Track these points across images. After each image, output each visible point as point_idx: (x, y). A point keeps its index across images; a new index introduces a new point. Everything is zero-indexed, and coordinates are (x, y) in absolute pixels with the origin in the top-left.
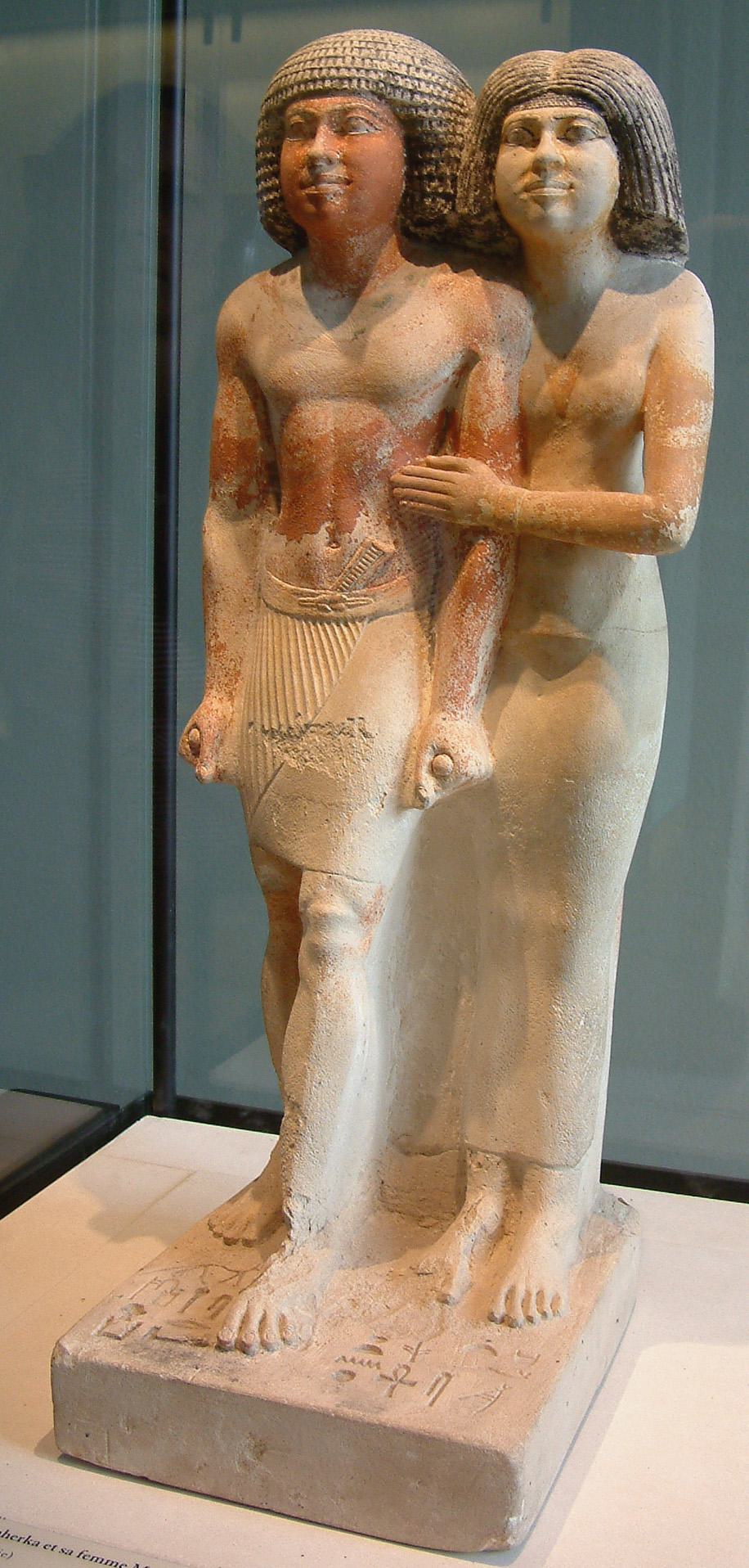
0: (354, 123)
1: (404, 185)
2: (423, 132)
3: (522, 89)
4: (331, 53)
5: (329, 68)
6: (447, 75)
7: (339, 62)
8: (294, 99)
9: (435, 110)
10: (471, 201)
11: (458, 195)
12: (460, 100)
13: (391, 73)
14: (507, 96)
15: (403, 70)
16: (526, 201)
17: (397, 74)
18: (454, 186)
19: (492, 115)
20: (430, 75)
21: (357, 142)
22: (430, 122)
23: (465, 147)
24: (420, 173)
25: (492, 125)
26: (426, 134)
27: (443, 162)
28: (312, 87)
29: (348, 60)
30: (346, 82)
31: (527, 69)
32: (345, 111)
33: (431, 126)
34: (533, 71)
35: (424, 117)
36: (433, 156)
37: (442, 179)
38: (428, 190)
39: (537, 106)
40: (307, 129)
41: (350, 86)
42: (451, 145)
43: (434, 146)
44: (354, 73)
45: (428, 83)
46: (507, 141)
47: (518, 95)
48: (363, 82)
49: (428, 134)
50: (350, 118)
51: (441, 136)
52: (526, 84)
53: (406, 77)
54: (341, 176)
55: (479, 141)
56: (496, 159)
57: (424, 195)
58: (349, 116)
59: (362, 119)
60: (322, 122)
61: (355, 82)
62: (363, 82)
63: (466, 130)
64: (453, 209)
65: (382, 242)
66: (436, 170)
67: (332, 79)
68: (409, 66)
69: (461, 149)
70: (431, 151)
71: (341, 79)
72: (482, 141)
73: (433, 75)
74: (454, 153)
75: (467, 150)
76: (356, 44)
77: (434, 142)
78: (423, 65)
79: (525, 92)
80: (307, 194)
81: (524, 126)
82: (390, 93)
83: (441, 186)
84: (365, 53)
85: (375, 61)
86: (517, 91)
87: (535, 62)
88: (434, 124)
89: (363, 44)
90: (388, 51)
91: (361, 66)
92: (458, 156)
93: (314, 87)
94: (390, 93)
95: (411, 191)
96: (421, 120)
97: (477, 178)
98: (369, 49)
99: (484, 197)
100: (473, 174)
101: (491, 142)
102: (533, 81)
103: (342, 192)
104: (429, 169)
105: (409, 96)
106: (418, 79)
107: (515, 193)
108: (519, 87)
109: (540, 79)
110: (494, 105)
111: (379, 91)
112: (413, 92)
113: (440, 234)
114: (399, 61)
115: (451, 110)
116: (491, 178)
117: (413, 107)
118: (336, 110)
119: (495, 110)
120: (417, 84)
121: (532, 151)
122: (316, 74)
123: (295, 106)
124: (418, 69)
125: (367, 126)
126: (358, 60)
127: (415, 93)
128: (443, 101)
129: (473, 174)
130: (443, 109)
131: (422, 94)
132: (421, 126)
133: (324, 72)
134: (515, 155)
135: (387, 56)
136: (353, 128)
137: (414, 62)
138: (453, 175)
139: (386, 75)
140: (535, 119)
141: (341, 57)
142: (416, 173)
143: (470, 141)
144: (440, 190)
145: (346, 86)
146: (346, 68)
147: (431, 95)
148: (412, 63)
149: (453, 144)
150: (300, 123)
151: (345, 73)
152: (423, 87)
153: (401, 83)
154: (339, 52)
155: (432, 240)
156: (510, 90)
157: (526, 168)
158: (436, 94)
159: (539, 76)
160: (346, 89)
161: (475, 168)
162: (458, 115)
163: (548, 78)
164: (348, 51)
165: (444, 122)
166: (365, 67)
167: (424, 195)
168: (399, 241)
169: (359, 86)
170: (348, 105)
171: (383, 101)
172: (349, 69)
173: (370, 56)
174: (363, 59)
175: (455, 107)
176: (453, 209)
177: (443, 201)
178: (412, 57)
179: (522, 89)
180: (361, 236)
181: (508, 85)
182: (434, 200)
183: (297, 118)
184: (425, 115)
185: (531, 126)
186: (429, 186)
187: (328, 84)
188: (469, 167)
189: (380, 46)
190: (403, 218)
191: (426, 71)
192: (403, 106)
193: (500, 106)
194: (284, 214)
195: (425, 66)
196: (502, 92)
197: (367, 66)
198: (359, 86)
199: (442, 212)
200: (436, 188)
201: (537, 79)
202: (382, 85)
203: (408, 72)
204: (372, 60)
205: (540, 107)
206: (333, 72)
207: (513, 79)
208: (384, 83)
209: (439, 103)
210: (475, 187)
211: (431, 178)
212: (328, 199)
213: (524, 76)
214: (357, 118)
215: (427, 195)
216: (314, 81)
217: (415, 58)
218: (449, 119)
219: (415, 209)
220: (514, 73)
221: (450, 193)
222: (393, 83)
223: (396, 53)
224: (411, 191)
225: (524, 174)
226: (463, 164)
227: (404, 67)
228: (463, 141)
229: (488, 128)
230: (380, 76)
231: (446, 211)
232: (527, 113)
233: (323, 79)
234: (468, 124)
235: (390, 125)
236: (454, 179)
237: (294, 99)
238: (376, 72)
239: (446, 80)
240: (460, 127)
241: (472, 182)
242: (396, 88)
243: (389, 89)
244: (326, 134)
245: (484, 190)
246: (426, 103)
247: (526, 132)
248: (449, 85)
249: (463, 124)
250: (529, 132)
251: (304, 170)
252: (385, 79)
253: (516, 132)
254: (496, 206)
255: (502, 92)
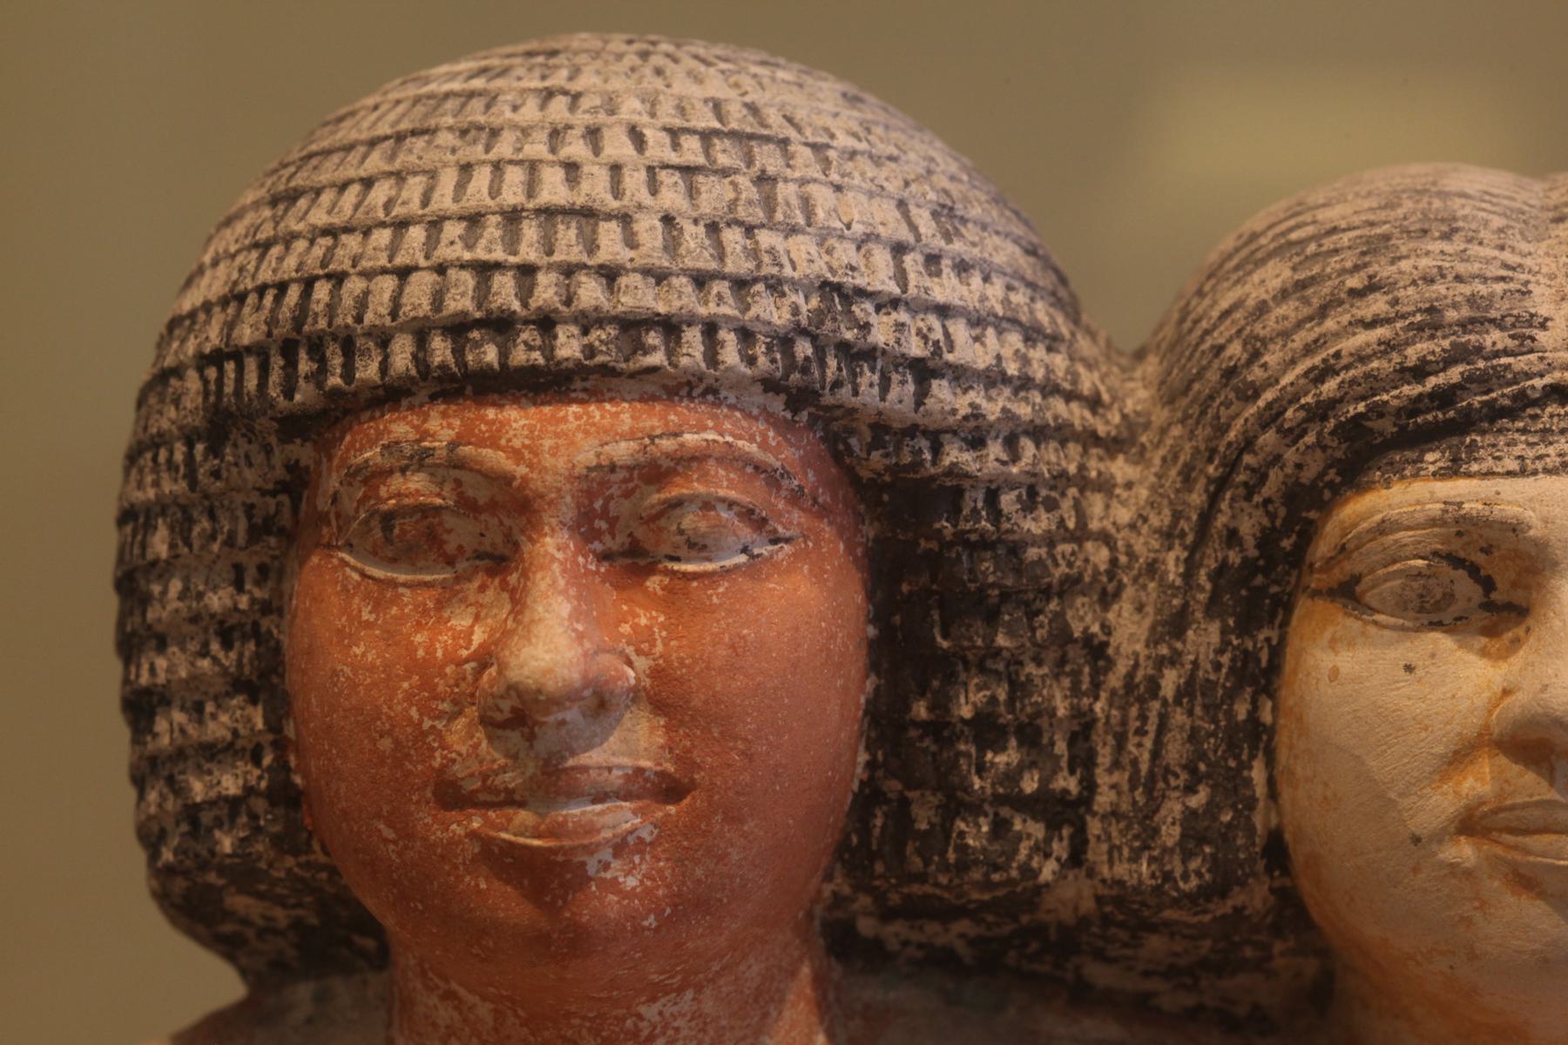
0: (691, 520)
1: (863, 757)
2: (961, 538)
3: (1432, 382)
4: (554, 190)
5: (569, 270)
6: (1025, 263)
7: (610, 242)
8: (391, 395)
9: (1011, 443)
10: (1171, 834)
11: (1104, 799)
12: (1088, 382)
13: (838, 288)
14: (1361, 407)
15: (880, 277)
16: (1468, 874)
17: (861, 293)
18: (1083, 761)
19: (1275, 477)
20: (976, 280)
21: (713, 609)
22: (992, 497)
23: (1129, 592)
24: (941, 705)
25: (1272, 516)
26: (967, 544)
27: (1039, 662)
28: (491, 354)
29: (649, 229)
30: (653, 338)
31: (1440, 288)
32: (654, 472)
33: (996, 514)
34: (1472, 300)
35: (967, 476)
36: (1002, 640)
37: (1030, 736)
38: (977, 783)
39: (1513, 465)
40: (460, 532)
41: (670, 354)
42: (1071, 586)
43: (1005, 596)
44: (680, 298)
45: (978, 322)
46: (1348, 593)
47: (1414, 407)
48: (728, 338)
49: (985, 544)
50: (678, 503)
51: (1032, 553)
52: (1448, 361)
53: (895, 303)
54: (645, 763)
55: (1202, 577)
56: (1277, 652)
57: (957, 804)
58: (673, 492)
59: (731, 504)
60: (549, 520)
61: (693, 338)
62: (728, 338)
63: (1124, 515)
64: (1077, 857)
65: (766, 998)
66: (1011, 700)
67: (587, 322)
68: (899, 249)
69: (1107, 599)
70: (992, 618)
71: (633, 326)
72: (1215, 576)
73: (986, 279)
74: (1082, 617)
75: (1140, 608)
76: (659, 148)
77: (1009, 582)
78: (948, 237)
79: (1444, 397)
80: (473, 835)
81: (1456, 546)
82: (837, 384)
83: (1033, 765)
84: (713, 194)
85: (765, 238)
86: (1410, 390)
87: (1463, 256)
88: (1008, 501)
89: (692, 151)
90: (803, 182)
91: (713, 265)
92: (1095, 628)
93: (504, 354)
94: (837, 384)
95: (893, 786)
96: (951, 490)
97: (1194, 736)
98: (725, 173)
99: (1226, 817)
100: (1179, 717)
101: (1259, 580)
102: (1479, 349)
103: (646, 834)
104: (980, 697)
105: (911, 387)
106: (943, 311)
107: (1417, 840)
108: (1419, 372)
109: (1511, 344)
110: (1293, 435)
111: (795, 377)
112: (923, 372)
113: (972, 942)
114: (858, 229)
115: (1062, 433)
116: (1258, 737)
117: (925, 433)
118: (613, 468)
119: (1290, 455)
120: (938, 335)
121: (1484, 653)
122: (505, 290)
123: (401, 428)
124: (932, 261)
125: (746, 534)
126: (693, 236)
127: (936, 374)
128: (1037, 397)
129: (1179, 717)
130: (1039, 433)
131: (961, 376)
132: (955, 512)
133: (546, 291)
134: (1409, 668)
135: (807, 205)
136: (691, 545)
137: (913, 228)
138: (1076, 713)
139: (815, 302)
140: (1515, 528)
141: (609, 217)
142: (921, 710)
143: (1152, 568)
144: (1030, 785)
145: (657, 358)
146: (646, 272)
147: (993, 378)
148: (911, 239)
149: (1078, 579)
150: (438, 510)
151: (638, 296)
152: (969, 351)
153: (881, 333)
154: (595, 187)
155: (942, 960)
156: (1375, 383)
157: (1471, 732)
158: (1012, 369)
159: (1498, 324)
160: (653, 370)
161: (1180, 694)
162: (1085, 452)
163: (1541, 336)
164: (635, 182)
165: (1044, 492)
166: (730, 267)
167: (957, 804)
168: (819, 980)
169: (712, 357)
170: (667, 444)
171: (804, 416)
172: (660, 277)
173: (741, 213)
174: (713, 228)
175: (1077, 414)
176: (1077, 857)
177: (1037, 830)
178: (902, 204)
179: (1432, 382)
180: (689, 994)
181: (1361, 358)
182: (1000, 828)
183: (416, 484)
184: (973, 467)
185: (1487, 551)
186: (981, 769)
187: (568, 346)
188: (1154, 686)
189: (766, 156)
190: (846, 890)
191: (962, 267)
192: (882, 430)
193: (1320, 445)
194: (290, 861)
195: (957, 246)
196: (1330, 387)
197: (737, 264)
198: (712, 357)
199: (1036, 874)
200: (1012, 776)
201: (1495, 338)
202: (804, 348)
203: (901, 277)
204: (749, 230)
205: (1523, 472)
206: (590, 292)
207: (1382, 332)
208: (814, 339)
209: (1023, 411)
210: (1184, 776)
211: (987, 730)
212: (592, 869)
213: (1432, 321)
214: (707, 505)
215: (975, 810)
216: (501, 325)
217: (914, 211)
218: (1063, 474)
219: (917, 863)
220: (1377, 305)
221: (1065, 791)
222: (849, 335)
223: (838, 188)
224: (893, 786)
225: (1460, 756)
226: (1122, 667)
227: (882, 258)
228: (1114, 562)
229: (1248, 527)
230: (795, 311)
231: (1048, 870)
232: (1468, 492)
233: (546, 323)
234: (1129, 485)
235: (823, 512)
236: (1082, 730)
237: (391, 395)
238: (776, 286)
239: (1029, 292)
240: (1096, 504)
241: (1175, 751)
242: (857, 355)
243: (832, 363)
244: (575, 576)
245: (1232, 786)
246: (976, 414)
247: (1461, 573)
248: (1042, 313)
249: (1105, 486)
250: (1473, 570)
251: (460, 724)
252: (819, 316)
253: (1420, 574)
254: (1276, 850)
255: (1330, 387)
